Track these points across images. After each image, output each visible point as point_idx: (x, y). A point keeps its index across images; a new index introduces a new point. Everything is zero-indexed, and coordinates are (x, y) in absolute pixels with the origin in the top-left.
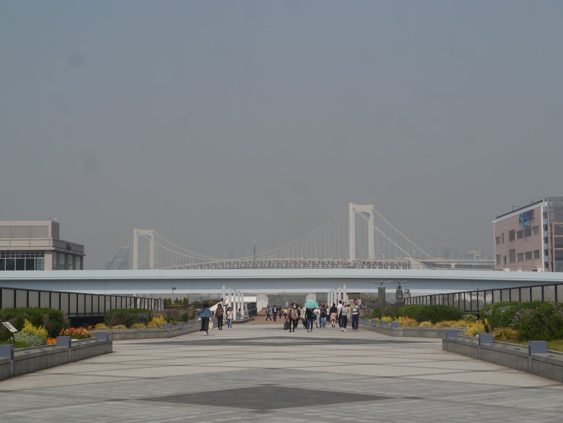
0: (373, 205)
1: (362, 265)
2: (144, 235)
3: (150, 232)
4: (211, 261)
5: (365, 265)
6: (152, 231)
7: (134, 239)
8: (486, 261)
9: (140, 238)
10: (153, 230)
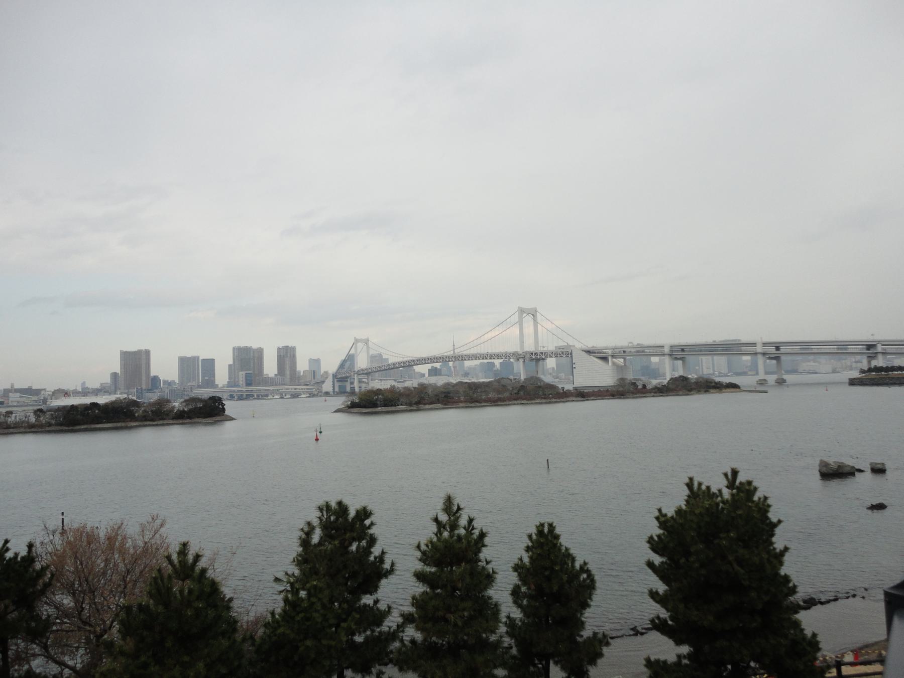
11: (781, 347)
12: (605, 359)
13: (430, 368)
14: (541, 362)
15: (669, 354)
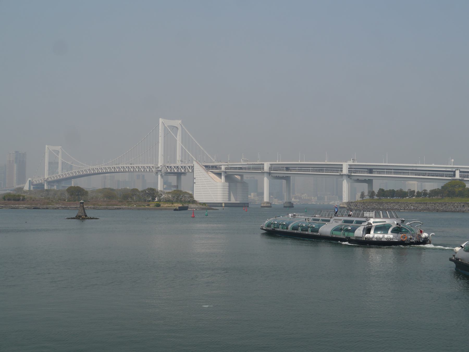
0: (181, 120)
1: (167, 169)
2: (52, 150)
3: (58, 148)
4: (84, 168)
6: (60, 147)
7: (46, 153)
8: (246, 163)
10: (61, 146)
11: (374, 170)
12: (219, 175)
14: (183, 177)
15: (267, 172)
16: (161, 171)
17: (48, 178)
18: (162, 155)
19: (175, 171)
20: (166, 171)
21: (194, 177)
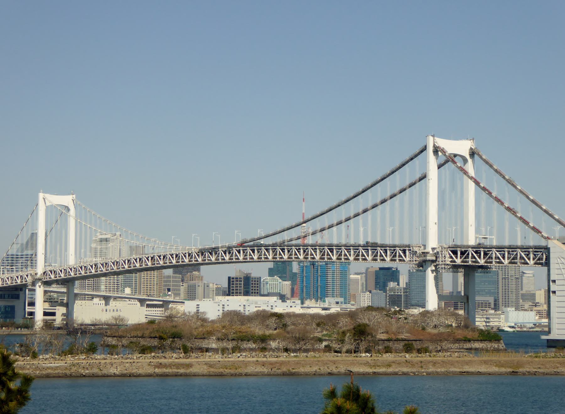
1: (451, 257)
3: (67, 200)
5: (457, 257)
6: (70, 197)
9: (50, 209)
10: (74, 196)
13: (233, 275)
14: (478, 275)
16: (433, 261)
17: (44, 273)
18: (436, 223)
19: (479, 263)
20: (449, 263)
21: (552, 278)
